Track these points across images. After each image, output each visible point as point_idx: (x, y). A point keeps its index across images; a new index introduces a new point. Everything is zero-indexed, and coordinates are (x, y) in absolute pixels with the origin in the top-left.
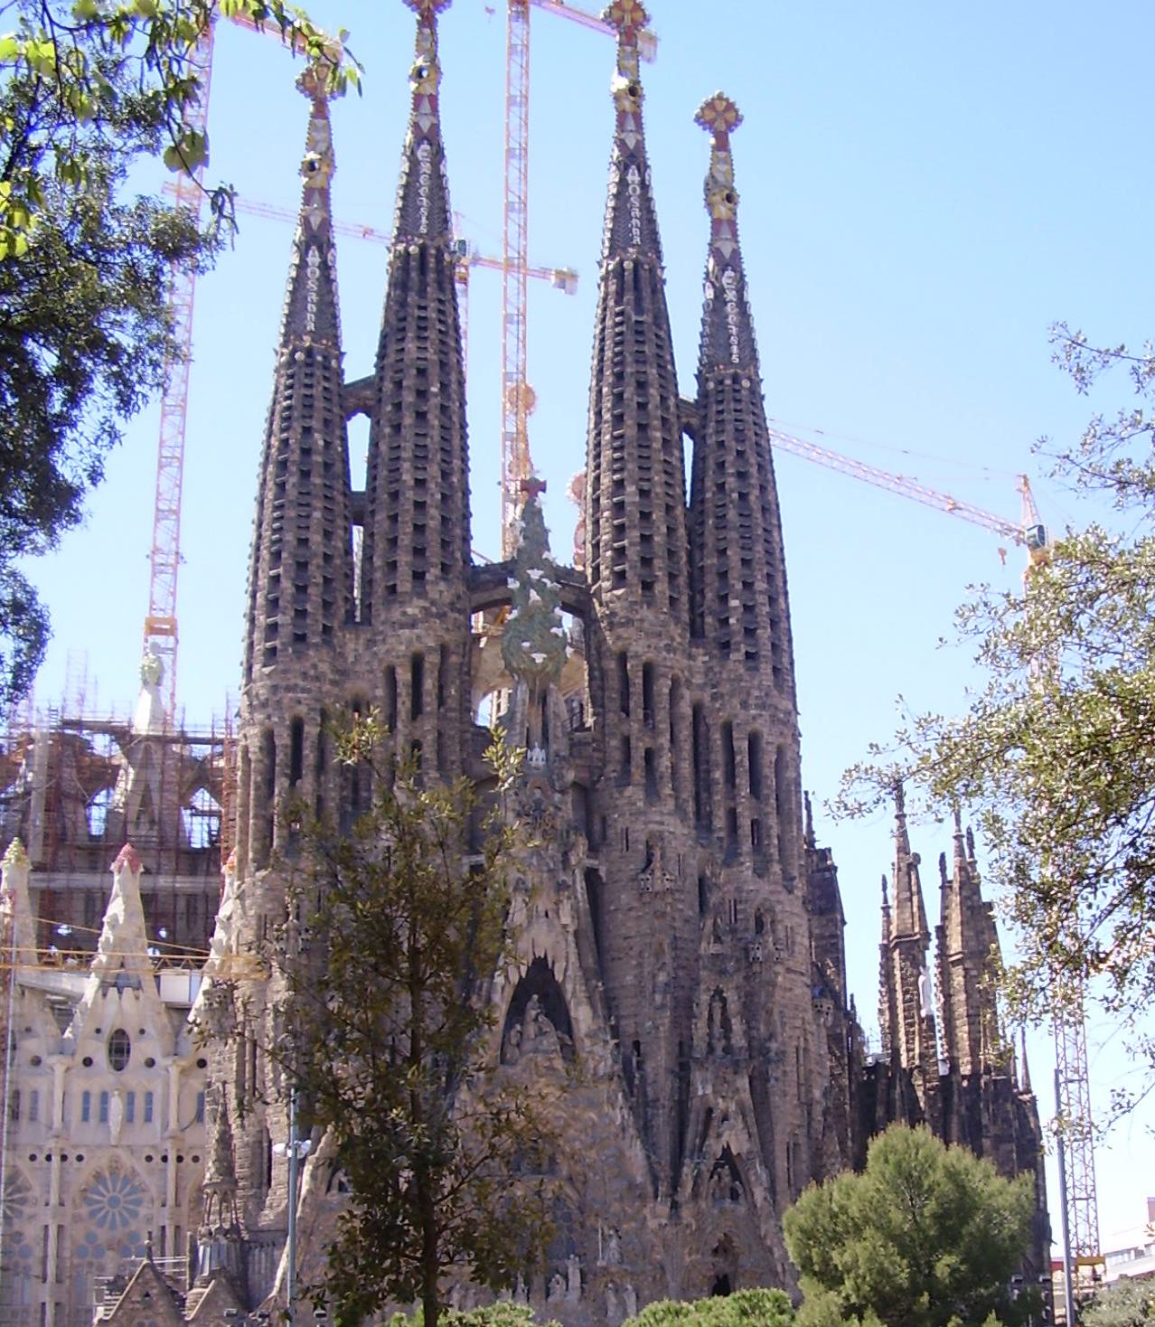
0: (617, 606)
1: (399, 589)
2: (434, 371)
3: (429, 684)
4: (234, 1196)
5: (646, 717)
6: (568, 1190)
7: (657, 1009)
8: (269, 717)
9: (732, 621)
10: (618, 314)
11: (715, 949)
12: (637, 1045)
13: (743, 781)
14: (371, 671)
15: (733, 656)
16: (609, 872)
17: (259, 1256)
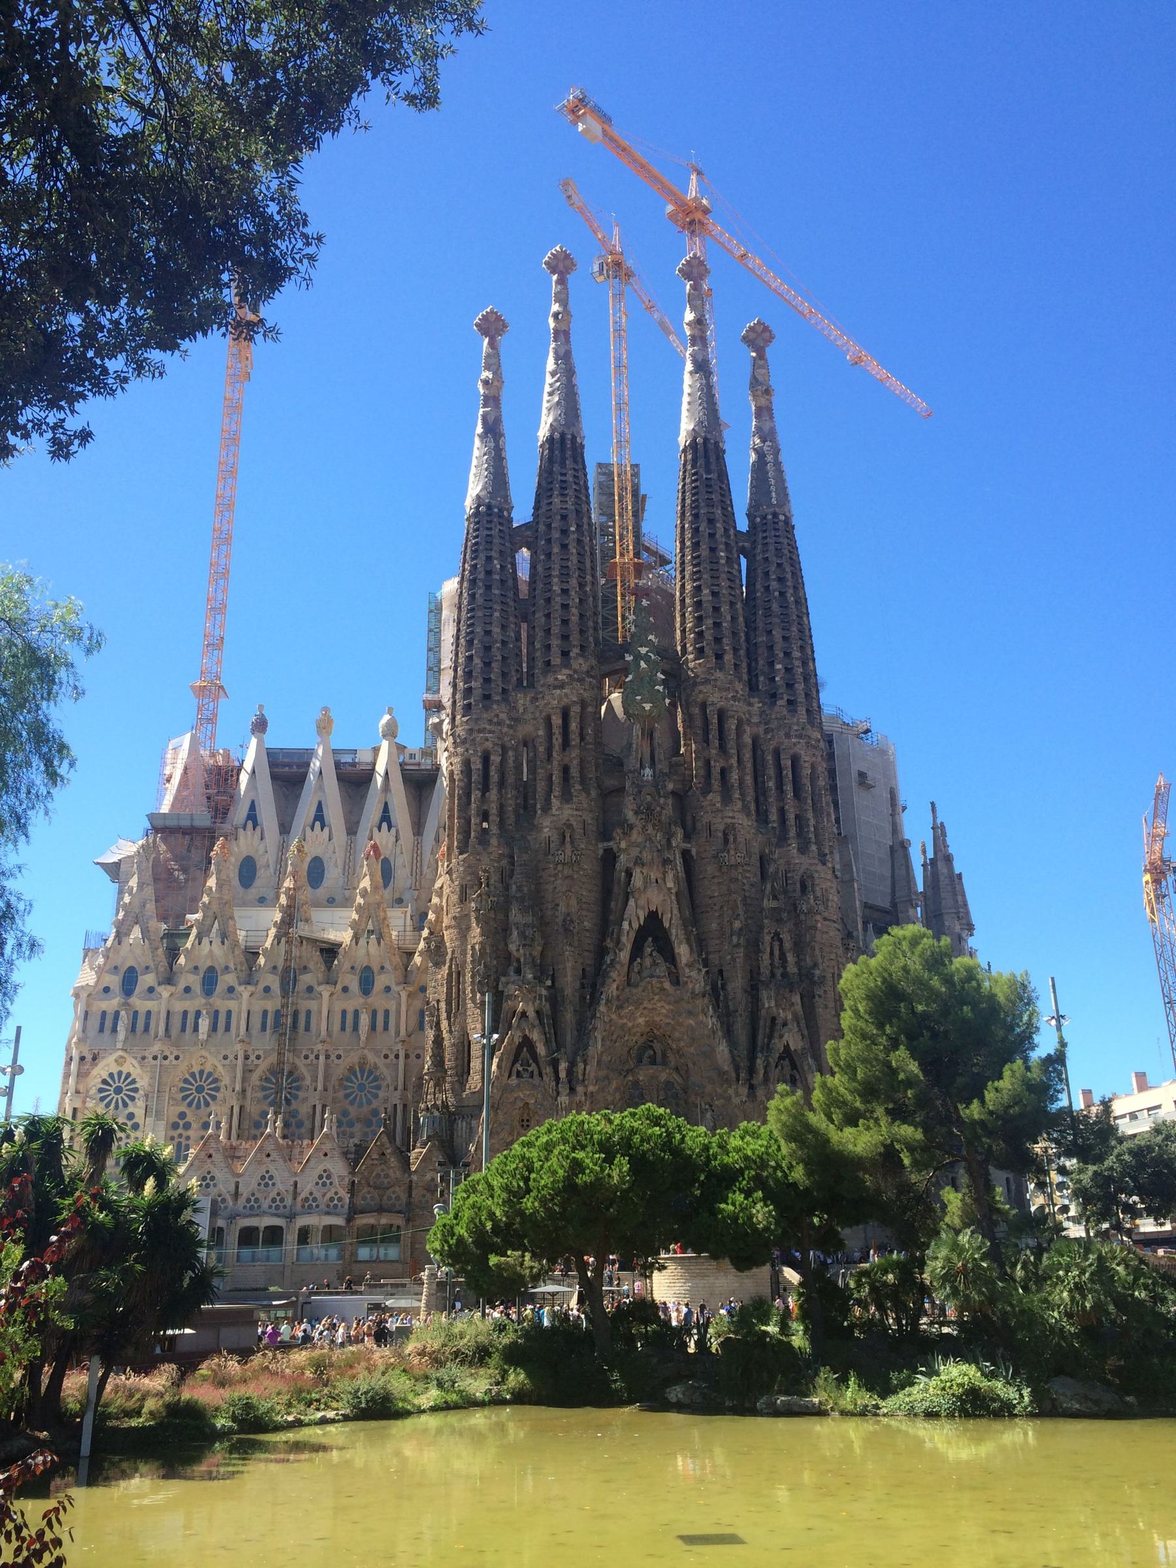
0: (699, 670)
1: (553, 663)
2: (572, 517)
3: (574, 726)
4: (444, 1082)
5: (721, 745)
6: (676, 1076)
7: (735, 946)
8: (467, 750)
9: (777, 679)
10: (694, 474)
11: (774, 904)
12: (721, 972)
13: (789, 788)
14: (535, 719)
15: (779, 703)
16: (698, 853)
17: (461, 1125)
